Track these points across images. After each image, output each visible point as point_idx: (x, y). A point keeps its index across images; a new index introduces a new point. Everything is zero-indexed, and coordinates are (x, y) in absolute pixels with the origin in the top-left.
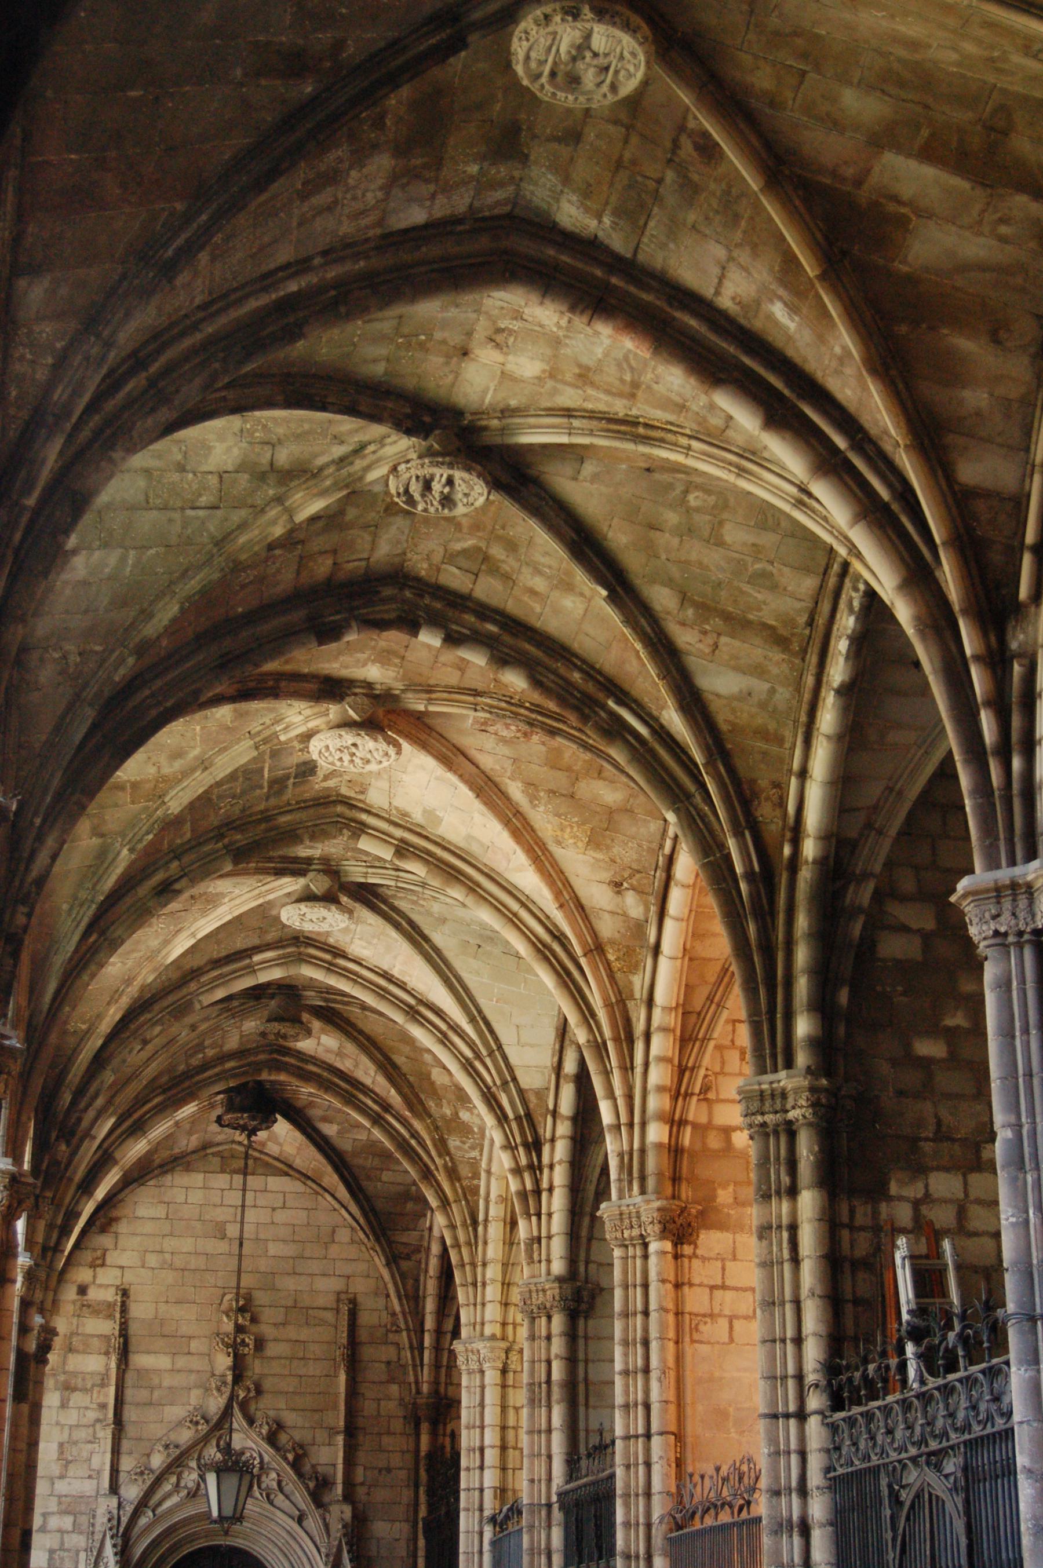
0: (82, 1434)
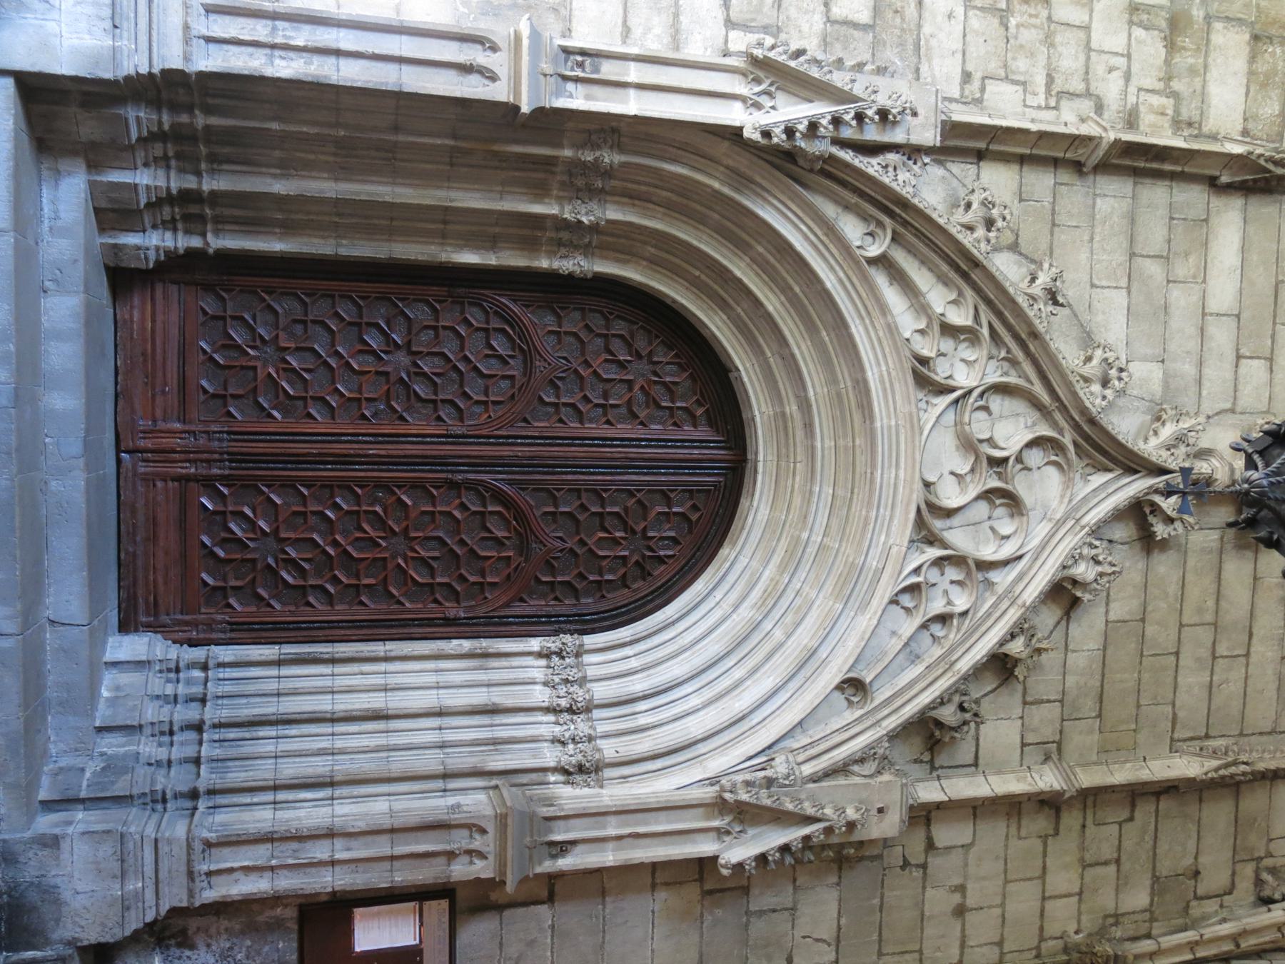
0: (1069, 60)
